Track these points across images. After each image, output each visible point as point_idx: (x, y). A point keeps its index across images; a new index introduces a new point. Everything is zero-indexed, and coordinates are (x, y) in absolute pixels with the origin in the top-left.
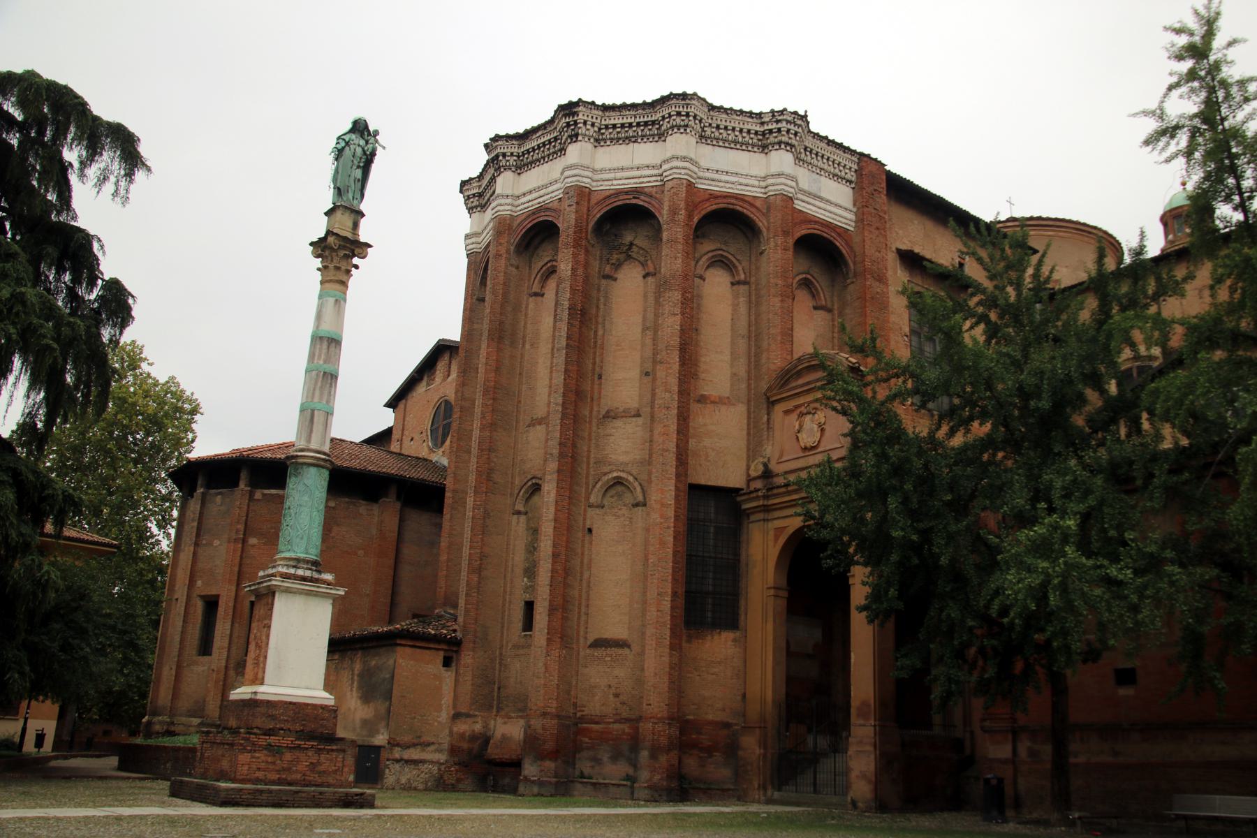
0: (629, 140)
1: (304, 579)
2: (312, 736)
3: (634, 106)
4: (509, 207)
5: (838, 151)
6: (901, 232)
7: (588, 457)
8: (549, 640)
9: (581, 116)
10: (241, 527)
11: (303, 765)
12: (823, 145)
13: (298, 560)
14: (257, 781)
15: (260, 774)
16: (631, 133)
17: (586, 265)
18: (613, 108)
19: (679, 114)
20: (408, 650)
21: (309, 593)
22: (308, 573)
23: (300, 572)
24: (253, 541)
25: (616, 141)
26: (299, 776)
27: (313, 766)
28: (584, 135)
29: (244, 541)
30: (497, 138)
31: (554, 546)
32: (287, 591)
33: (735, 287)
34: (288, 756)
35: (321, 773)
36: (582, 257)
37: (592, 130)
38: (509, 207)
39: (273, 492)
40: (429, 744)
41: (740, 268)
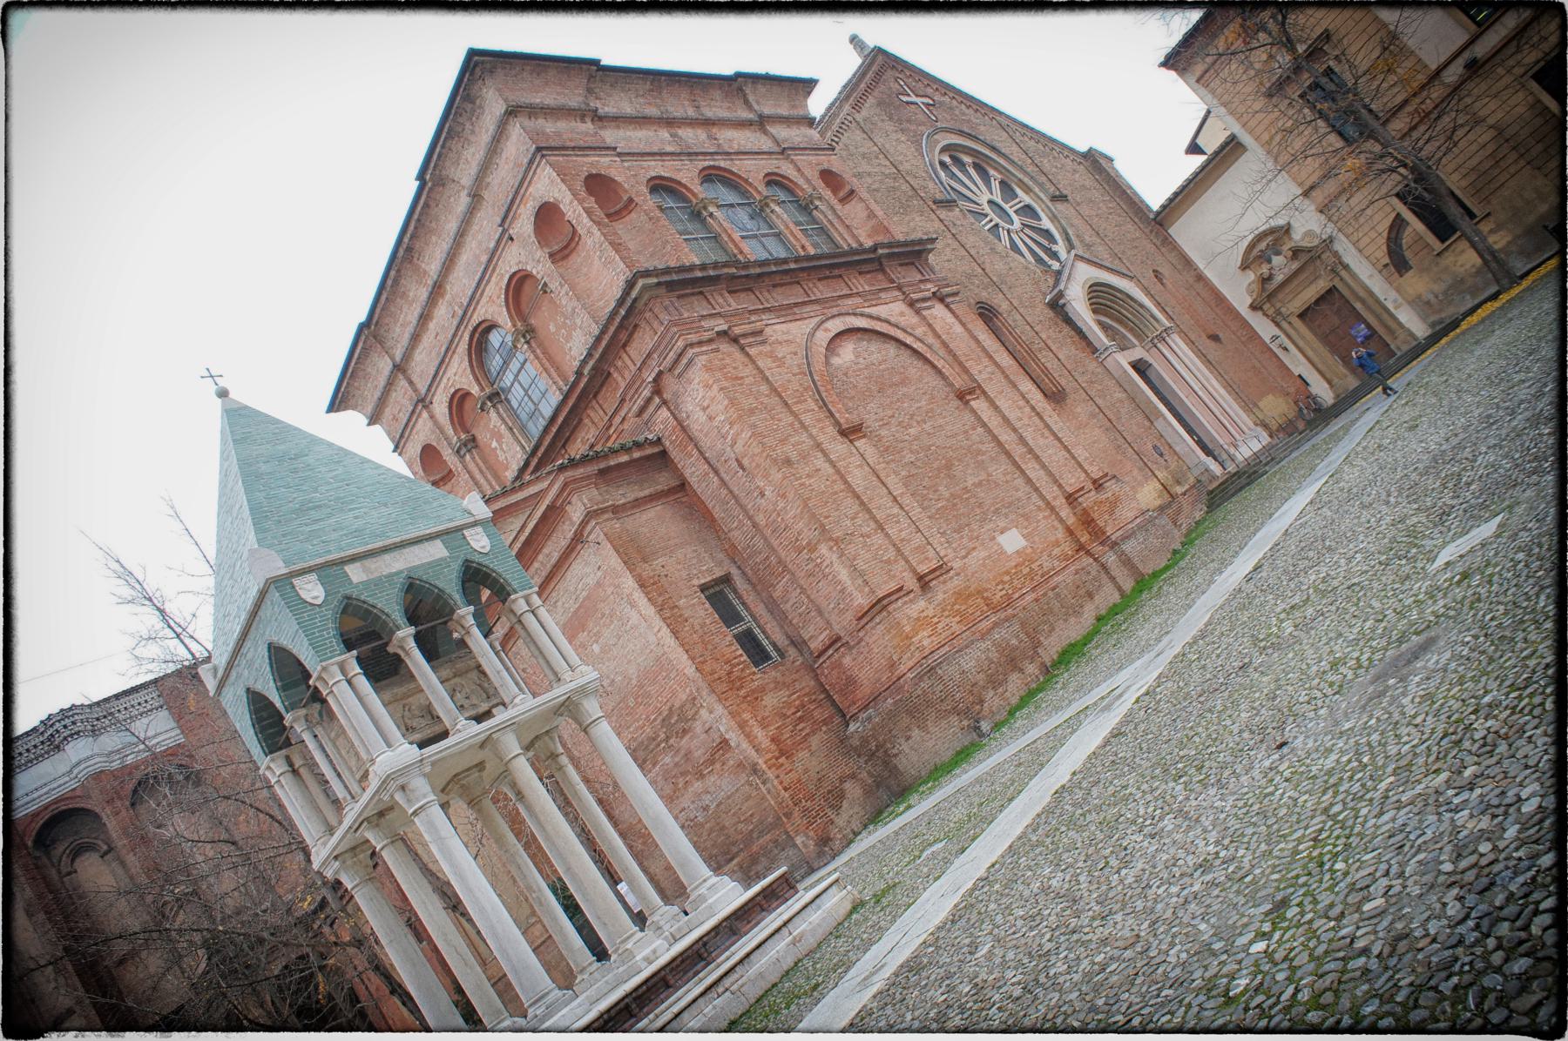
33: (106, 858)
41: (100, 842)
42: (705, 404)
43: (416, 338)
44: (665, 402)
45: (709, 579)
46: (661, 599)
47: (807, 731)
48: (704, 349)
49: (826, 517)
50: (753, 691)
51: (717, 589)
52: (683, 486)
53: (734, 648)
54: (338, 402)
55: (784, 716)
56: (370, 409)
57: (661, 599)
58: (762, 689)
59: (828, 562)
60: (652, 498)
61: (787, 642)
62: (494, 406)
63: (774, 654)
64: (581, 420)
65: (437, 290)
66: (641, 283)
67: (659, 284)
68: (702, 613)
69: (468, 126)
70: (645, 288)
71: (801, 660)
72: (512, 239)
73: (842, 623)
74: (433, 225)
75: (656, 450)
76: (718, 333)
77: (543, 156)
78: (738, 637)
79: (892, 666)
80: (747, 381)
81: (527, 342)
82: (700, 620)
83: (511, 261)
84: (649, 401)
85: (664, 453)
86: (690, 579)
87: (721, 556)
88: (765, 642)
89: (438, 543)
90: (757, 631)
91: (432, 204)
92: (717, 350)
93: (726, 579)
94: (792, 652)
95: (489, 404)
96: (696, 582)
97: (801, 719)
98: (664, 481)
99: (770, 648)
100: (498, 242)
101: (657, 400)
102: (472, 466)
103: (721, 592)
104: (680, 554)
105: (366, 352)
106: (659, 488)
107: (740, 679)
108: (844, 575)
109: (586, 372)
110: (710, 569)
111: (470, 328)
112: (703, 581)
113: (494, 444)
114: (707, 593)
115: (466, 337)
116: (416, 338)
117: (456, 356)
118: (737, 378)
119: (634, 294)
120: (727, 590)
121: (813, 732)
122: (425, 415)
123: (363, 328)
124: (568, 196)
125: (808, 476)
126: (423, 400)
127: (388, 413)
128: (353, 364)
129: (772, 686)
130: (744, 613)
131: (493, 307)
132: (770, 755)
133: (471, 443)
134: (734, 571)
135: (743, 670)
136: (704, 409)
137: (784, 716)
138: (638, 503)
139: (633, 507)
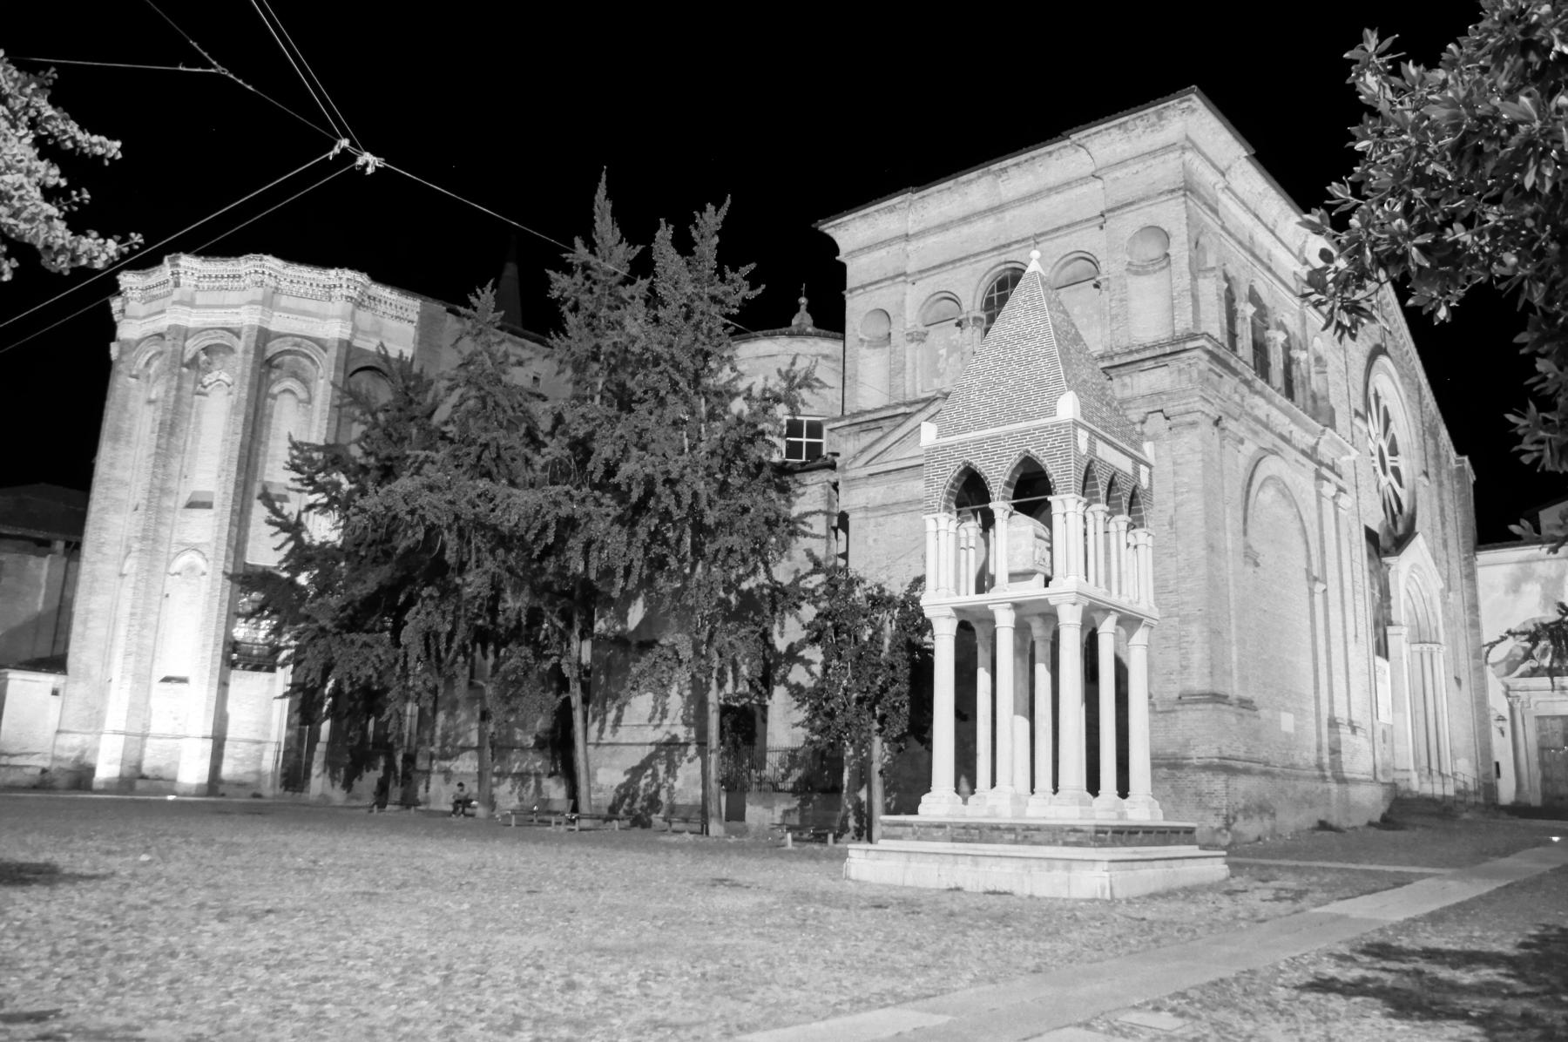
7: (171, 539)
8: (123, 678)
17: (179, 388)
31: (133, 607)
36: (174, 383)
40: (34, 754)
42: (1179, 461)
43: (943, 227)
59: (1189, 639)
65: (996, 209)
66: (1202, 342)
67: (1208, 352)
69: (1140, 130)
70: (1203, 348)
72: (1101, 228)
74: (1041, 169)
77: (1185, 195)
79: (1186, 744)
83: (1089, 239)
91: (1055, 155)
100: (1088, 220)
111: (1003, 258)
113: (943, 352)
116: (943, 227)
119: (1189, 345)
124: (1185, 238)
136: (1175, 463)
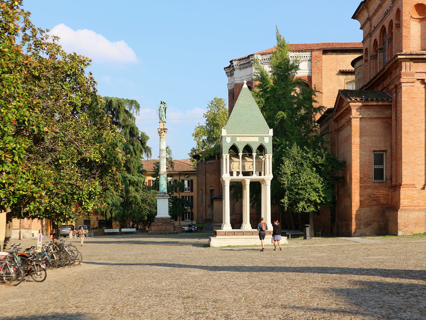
0: (246, 67)
1: (162, 196)
2: (166, 223)
3: (244, 59)
4: (230, 87)
5: (303, 53)
6: (342, 64)
9: (234, 64)
10: (204, 171)
11: (163, 228)
12: (297, 53)
13: (161, 193)
14: (156, 231)
15: (156, 230)
16: (246, 66)
18: (243, 59)
19: (252, 60)
20: (216, 202)
21: (163, 198)
22: (163, 195)
23: (161, 195)
24: (208, 175)
25: (244, 68)
26: (163, 230)
27: (165, 228)
28: (236, 69)
29: (206, 175)
30: (225, 69)
32: (159, 198)
34: (160, 227)
35: (167, 229)
37: (237, 66)
38: (230, 87)
39: (211, 161)
44: (396, 92)
45: (378, 149)
46: (356, 150)
47: (375, 204)
48: (409, 84)
49: (406, 154)
50: (366, 186)
51: (380, 153)
52: (391, 118)
53: (370, 172)
54: (354, 17)
55: (370, 197)
56: (363, 22)
57: (356, 150)
58: (369, 187)
60: (377, 118)
61: (389, 178)
62: (380, 52)
63: (385, 179)
64: (386, 78)
68: (367, 158)
71: (390, 184)
73: (398, 184)
75: (388, 104)
76: (418, 80)
78: (375, 169)
80: (417, 100)
81: (388, 42)
82: (365, 160)
84: (393, 89)
85: (391, 105)
86: (372, 147)
87: (388, 144)
88: (385, 175)
89: (258, 138)
90: (385, 170)
92: (413, 86)
93: (385, 151)
94: (389, 181)
95: (379, 51)
96: (373, 149)
97: (375, 200)
98: (387, 113)
99: (385, 177)
101: (395, 90)
102: (371, 64)
103: (383, 154)
104: (374, 138)
105: (362, 9)
106: (382, 116)
107: (364, 181)
108: (401, 172)
109: (386, 68)
110: (380, 146)
112: (375, 149)
114: (375, 153)
115: (381, 27)
116: (374, 14)
117: (378, 29)
118: (413, 98)
120: (384, 155)
121: (376, 205)
122: (369, 39)
123: (362, 3)
125: (411, 139)
126: (371, 34)
127: (365, 28)
128: (359, 10)
129: (374, 187)
130: (385, 164)
131: (386, 24)
132: (356, 204)
133: (375, 57)
134: (389, 150)
135: (367, 179)
137: (370, 197)
138: (371, 118)
139: (369, 119)
